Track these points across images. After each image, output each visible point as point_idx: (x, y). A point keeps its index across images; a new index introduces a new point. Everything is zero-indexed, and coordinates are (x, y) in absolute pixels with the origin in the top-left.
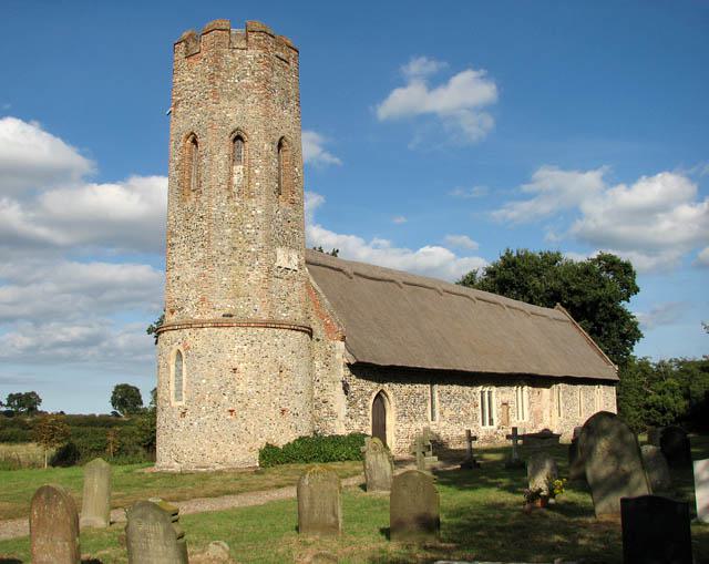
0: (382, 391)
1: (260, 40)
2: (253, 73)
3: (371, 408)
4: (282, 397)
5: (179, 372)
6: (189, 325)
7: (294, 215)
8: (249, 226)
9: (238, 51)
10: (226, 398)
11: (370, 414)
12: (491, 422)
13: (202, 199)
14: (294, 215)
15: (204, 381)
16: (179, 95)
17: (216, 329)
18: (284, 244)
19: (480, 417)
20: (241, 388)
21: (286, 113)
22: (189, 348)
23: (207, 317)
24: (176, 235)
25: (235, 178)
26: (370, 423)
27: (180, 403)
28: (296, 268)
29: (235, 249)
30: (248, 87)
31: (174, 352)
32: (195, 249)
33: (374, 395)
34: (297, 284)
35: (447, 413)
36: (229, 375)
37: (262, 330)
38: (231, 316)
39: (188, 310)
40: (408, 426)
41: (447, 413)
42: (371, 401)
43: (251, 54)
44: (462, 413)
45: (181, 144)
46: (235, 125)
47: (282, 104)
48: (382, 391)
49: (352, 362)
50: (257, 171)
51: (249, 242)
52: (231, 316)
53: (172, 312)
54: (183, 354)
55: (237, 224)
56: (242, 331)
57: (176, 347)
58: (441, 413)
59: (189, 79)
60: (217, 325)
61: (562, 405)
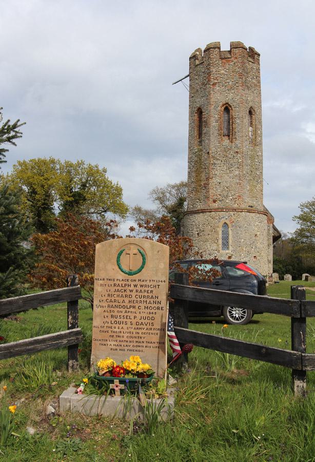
6: (234, 210)
8: (256, 160)
13: (237, 142)
15: (243, 240)
16: (216, 79)
17: (248, 213)
20: (258, 245)
23: (243, 206)
24: (217, 159)
27: (227, 251)
31: (221, 224)
32: (232, 169)
36: (254, 238)
45: (219, 108)
46: (251, 104)
52: (252, 207)
53: (214, 201)
56: (258, 215)
57: (223, 221)
59: (222, 72)
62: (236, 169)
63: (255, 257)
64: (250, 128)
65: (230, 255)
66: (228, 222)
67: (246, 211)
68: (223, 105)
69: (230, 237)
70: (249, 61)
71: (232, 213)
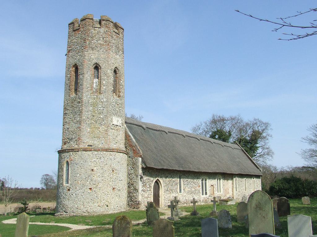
0: (158, 180)
1: (107, 24)
2: (103, 39)
3: (153, 187)
4: (114, 182)
5: (68, 170)
7: (120, 102)
9: (97, 29)
10: (88, 182)
11: (152, 190)
12: (206, 193)
14: (120, 102)
15: (78, 175)
17: (84, 152)
18: (116, 114)
19: (201, 191)
20: (95, 178)
21: (118, 57)
22: (72, 160)
25: (95, 84)
26: (152, 194)
27: (67, 185)
28: (121, 125)
29: (93, 116)
30: (100, 44)
33: (154, 181)
34: (121, 132)
35: (187, 189)
36: (90, 172)
37: (105, 152)
38: (91, 146)
39: (72, 143)
40: (169, 195)
41: (187, 189)
42: (153, 184)
43: (102, 30)
44: (193, 189)
46: (95, 61)
47: (116, 52)
48: (158, 180)
49: (144, 166)
50: (104, 82)
51: (100, 113)
52: (91, 146)
54: (69, 162)
55: (94, 105)
56: (96, 153)
58: (184, 190)
60: (85, 150)
61: (237, 186)
62: (78, 116)
63: (90, 189)
64: (96, 80)
65: (69, 188)
66: (69, 161)
67: (82, 150)
68: (74, 66)
69: (70, 172)
70: (95, 27)
71: (71, 153)
